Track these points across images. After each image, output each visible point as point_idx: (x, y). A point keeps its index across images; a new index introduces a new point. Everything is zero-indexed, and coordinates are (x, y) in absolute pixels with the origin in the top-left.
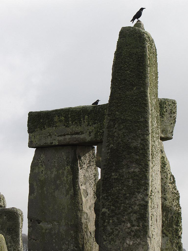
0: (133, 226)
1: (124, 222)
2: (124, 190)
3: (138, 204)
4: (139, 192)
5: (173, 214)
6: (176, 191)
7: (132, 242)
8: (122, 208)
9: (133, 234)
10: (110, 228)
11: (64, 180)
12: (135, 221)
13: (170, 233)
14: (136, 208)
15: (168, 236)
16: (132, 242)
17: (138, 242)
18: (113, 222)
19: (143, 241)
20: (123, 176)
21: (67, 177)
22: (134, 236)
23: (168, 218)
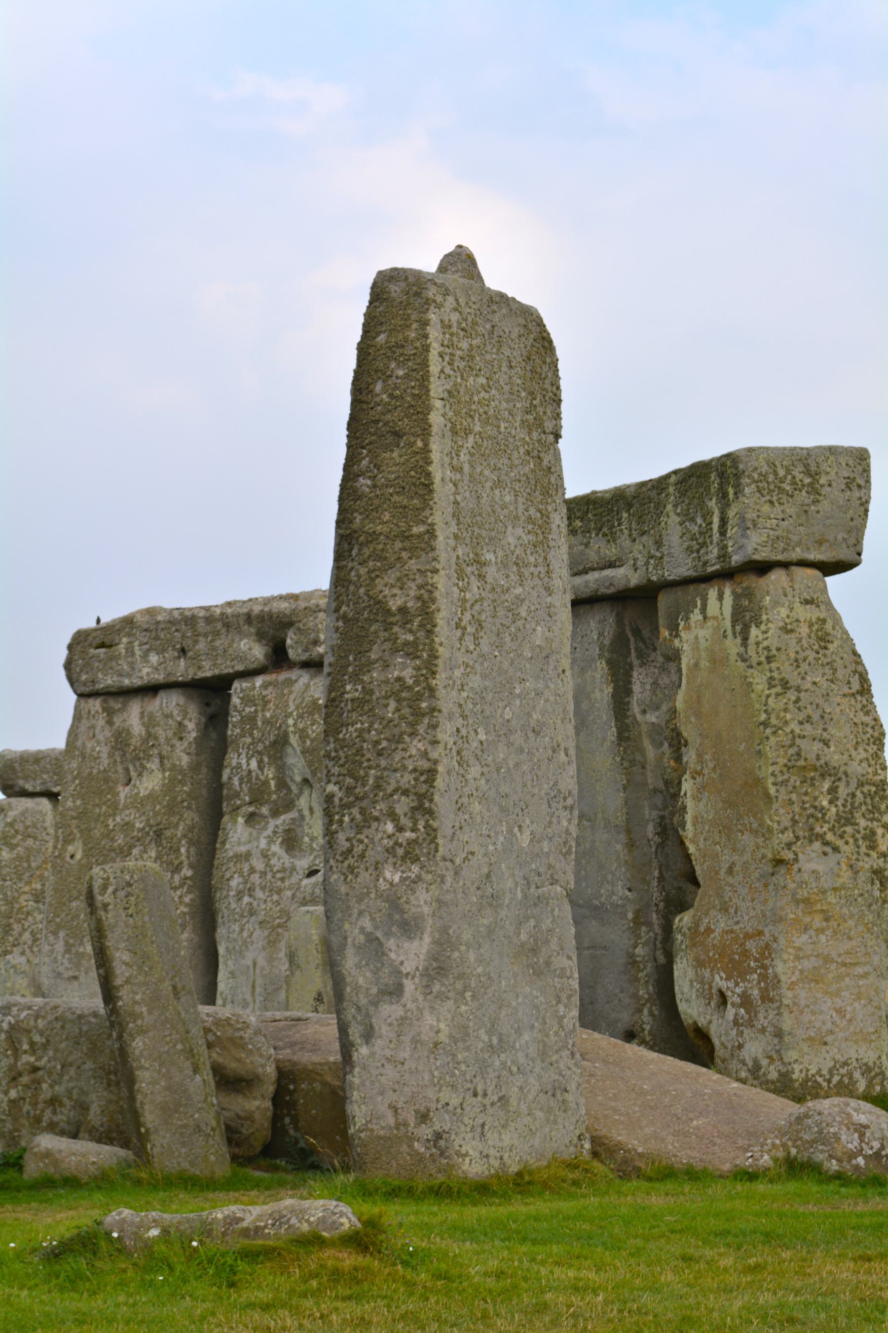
0: (400, 829)
1: (377, 819)
2: (376, 730)
3: (411, 767)
4: (413, 734)
5: (854, 783)
6: (868, 719)
7: (399, 874)
8: (371, 782)
9: (400, 852)
10: (344, 838)
11: (596, 699)
12: (405, 815)
13: (847, 843)
14: (407, 780)
15: (842, 849)
16: (399, 874)
17: (413, 876)
18: (352, 820)
19: (428, 872)
20: (371, 692)
21: (601, 691)
22: (403, 859)
23: (837, 799)
